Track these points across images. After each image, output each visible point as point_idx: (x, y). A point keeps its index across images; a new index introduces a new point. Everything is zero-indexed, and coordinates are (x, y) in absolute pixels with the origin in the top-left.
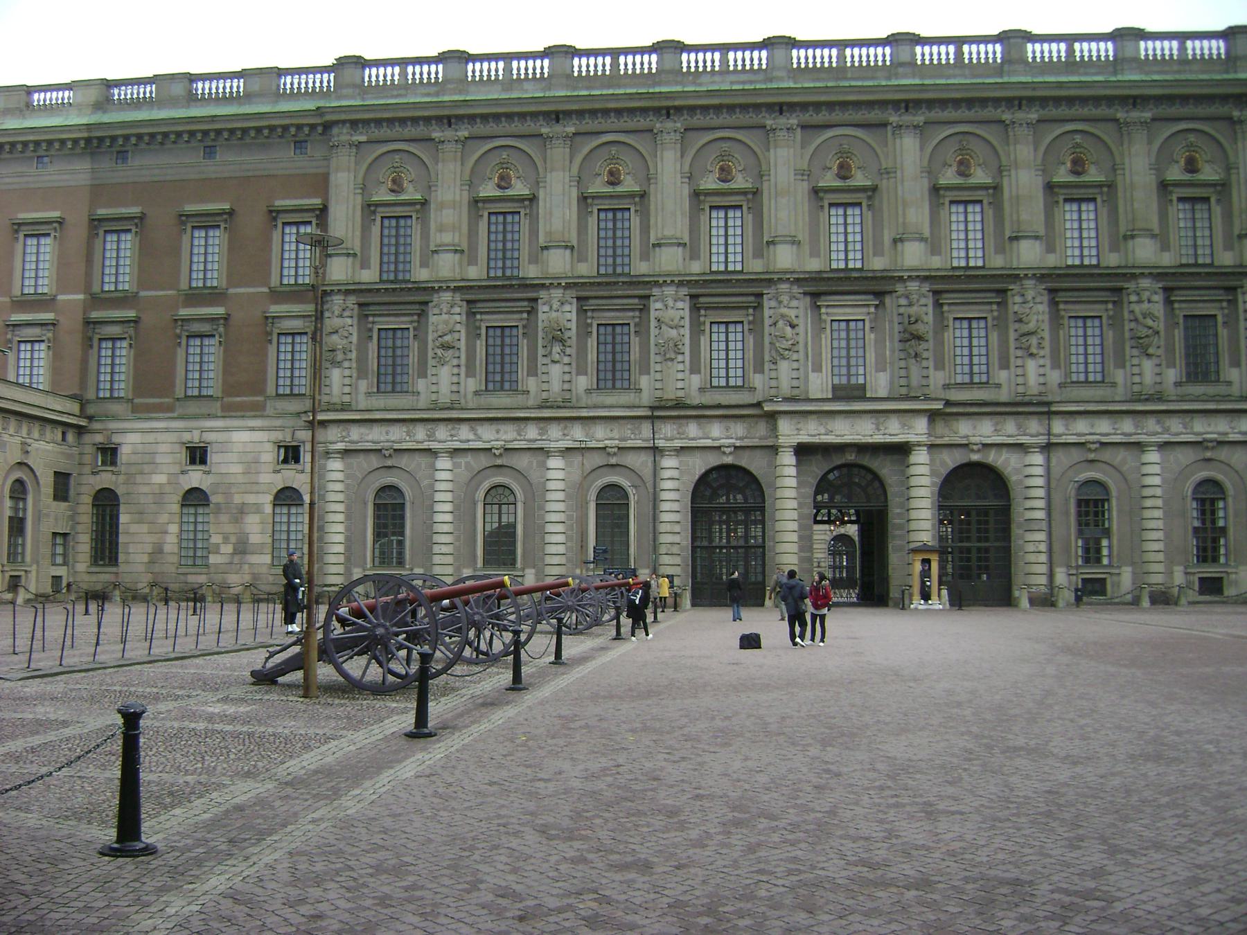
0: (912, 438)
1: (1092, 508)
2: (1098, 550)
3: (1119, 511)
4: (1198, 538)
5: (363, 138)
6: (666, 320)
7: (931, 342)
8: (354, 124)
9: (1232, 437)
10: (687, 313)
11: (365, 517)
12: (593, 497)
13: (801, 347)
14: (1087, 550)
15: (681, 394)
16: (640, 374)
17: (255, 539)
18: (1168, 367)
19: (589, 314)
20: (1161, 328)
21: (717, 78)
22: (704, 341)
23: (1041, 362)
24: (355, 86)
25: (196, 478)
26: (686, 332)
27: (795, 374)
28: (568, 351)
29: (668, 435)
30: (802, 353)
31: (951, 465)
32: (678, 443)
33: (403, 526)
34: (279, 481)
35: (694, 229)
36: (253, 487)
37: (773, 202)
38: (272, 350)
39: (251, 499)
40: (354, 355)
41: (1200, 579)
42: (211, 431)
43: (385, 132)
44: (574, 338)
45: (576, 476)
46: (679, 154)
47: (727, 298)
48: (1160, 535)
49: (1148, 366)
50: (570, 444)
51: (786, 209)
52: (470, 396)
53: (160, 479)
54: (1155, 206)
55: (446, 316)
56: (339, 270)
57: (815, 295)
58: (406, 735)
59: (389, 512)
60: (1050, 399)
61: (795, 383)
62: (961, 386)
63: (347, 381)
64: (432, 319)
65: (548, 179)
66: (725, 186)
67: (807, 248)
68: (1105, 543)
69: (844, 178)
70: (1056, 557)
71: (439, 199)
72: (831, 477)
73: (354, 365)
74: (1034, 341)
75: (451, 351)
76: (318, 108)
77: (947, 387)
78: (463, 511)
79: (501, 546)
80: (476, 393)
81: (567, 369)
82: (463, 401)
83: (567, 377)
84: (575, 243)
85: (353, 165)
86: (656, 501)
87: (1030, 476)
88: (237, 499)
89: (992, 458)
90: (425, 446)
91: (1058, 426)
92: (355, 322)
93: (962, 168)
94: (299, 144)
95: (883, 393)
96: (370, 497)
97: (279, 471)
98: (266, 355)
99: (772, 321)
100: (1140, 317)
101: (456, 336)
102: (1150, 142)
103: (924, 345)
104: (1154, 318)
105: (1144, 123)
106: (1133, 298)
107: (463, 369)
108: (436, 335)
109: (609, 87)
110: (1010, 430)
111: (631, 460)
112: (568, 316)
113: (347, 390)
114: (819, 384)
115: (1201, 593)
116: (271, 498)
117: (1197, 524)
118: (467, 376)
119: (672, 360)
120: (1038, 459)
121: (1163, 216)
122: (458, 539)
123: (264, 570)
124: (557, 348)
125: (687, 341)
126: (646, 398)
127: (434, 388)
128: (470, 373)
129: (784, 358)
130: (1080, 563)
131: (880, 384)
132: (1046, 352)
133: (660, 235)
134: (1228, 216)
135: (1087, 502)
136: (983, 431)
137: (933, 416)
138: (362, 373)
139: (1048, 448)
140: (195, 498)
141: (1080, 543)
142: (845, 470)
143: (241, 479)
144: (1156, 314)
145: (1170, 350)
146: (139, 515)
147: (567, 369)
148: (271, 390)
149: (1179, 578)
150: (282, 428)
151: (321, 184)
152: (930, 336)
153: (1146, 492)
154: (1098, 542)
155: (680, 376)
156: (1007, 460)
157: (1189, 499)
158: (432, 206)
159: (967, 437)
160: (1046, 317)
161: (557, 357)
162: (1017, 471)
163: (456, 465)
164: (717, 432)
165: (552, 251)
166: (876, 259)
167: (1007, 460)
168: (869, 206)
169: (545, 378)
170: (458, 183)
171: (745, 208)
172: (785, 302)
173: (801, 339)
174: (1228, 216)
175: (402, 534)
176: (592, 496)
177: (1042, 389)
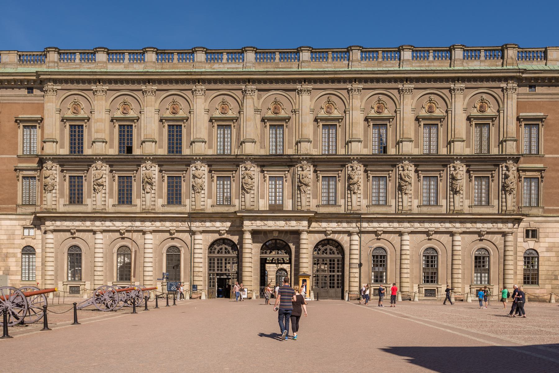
1: (379, 259)
2: (382, 277)
3: (390, 261)
4: (424, 272)
5: (59, 87)
6: (197, 175)
7: (312, 186)
9: (441, 230)
10: (206, 172)
11: (63, 259)
12: (165, 251)
13: (255, 188)
14: (376, 277)
15: (202, 207)
16: (186, 198)
17: (13, 268)
18: (415, 199)
19: (164, 172)
20: (413, 181)
21: (221, 66)
22: (214, 184)
23: (359, 196)
24: (55, 62)
26: (206, 180)
27: (252, 200)
28: (154, 188)
29: (196, 226)
30: (255, 192)
31: (319, 240)
33: (81, 262)
35: (210, 134)
36: (12, 245)
37: (245, 123)
38: (19, 184)
39: (11, 251)
40: (57, 187)
41: (425, 290)
43: (69, 86)
44: (157, 182)
45: (158, 243)
46: (203, 101)
47: (224, 165)
48: (408, 271)
50: (155, 229)
51: (251, 126)
52: (110, 207)
54: (413, 128)
55: (101, 171)
56: (50, 149)
57: (262, 166)
59: (75, 257)
60: (360, 212)
61: (252, 203)
62: (323, 206)
63: (54, 199)
64: (93, 172)
65: (145, 110)
66: (224, 116)
67: (258, 144)
68: (384, 274)
69: (276, 113)
70: (362, 280)
71: (96, 118)
72: (267, 244)
73: (58, 192)
74: (356, 186)
75: (101, 187)
76: (37, 72)
77: (318, 206)
78: (107, 257)
79: (125, 273)
80: (114, 206)
81: (153, 195)
82: (107, 209)
83: (153, 199)
84: (157, 140)
85: (54, 100)
86: (192, 253)
88: (4, 251)
89: (336, 237)
90: (90, 228)
91: (365, 225)
92: (58, 173)
93: (328, 110)
94: (30, 90)
95: (290, 208)
96: (66, 250)
97: (24, 239)
98: (17, 186)
99: (243, 176)
100: (403, 177)
101: (104, 180)
102: (413, 99)
103: (309, 188)
104: (409, 177)
105: (410, 90)
106: (401, 169)
107: (107, 196)
108: (95, 179)
109: (173, 68)
110: (344, 226)
111: (180, 235)
112: (154, 172)
113: (54, 203)
114: (263, 205)
115: (426, 296)
116: (21, 250)
117: (424, 266)
118: (109, 198)
119: (199, 192)
120: (356, 237)
122: (106, 269)
123: (18, 282)
124: (148, 186)
125: (206, 184)
126: (187, 209)
127: (94, 203)
128: (111, 196)
129: (248, 193)
130: (373, 281)
131: (288, 205)
132: (362, 192)
133: (195, 137)
135: (377, 257)
136: (333, 226)
137: (310, 220)
138: (62, 195)
141: (373, 274)
142: (274, 241)
143: (6, 242)
144: (410, 175)
145: (417, 191)
147: (153, 195)
148: (19, 202)
149: (416, 289)
150: (25, 219)
151: (41, 107)
152: (311, 184)
154: (382, 273)
155: (202, 199)
156: (343, 237)
157: (422, 256)
158: (93, 121)
159: (326, 228)
160: (362, 177)
161: (149, 190)
163: (105, 237)
164: (218, 224)
165: (146, 143)
166: (289, 150)
167: (343, 237)
168: (287, 126)
169: (144, 199)
170: (104, 110)
171: (232, 126)
172: (249, 168)
173: (256, 184)
175: (81, 267)
176: (164, 251)
177: (358, 208)
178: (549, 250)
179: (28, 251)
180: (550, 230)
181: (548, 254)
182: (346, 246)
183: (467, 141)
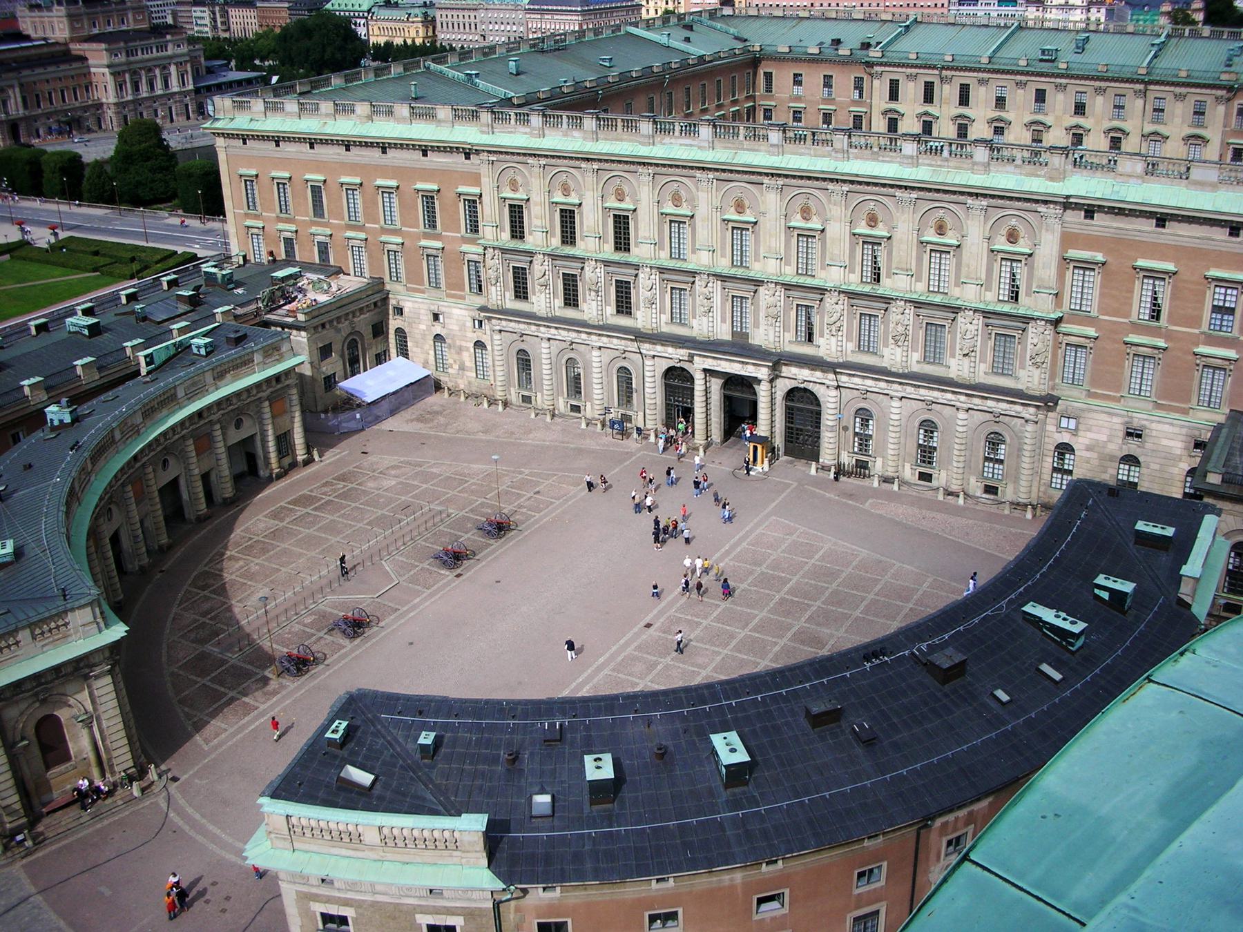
0: (760, 376)
8: (489, 152)
25: (438, 329)
32: (652, 353)
34: (475, 337)
36: (464, 338)
39: (464, 344)
42: (444, 306)
49: (899, 350)
53: (423, 327)
54: (914, 253)
58: (316, 661)
74: (834, 328)
78: (554, 368)
87: (828, 399)
88: (458, 343)
89: (810, 387)
120: (834, 393)
121: (919, 260)
134: (959, 266)
139: (838, 387)
140: (438, 338)
146: (417, 344)
153: (892, 422)
162: (824, 396)
164: (670, 350)
174: (959, 266)
176: (615, 371)
178: (1089, 448)
179: (479, 345)
180: (1095, 422)
181: (1088, 454)
182: (821, 400)
183: (985, 285)
